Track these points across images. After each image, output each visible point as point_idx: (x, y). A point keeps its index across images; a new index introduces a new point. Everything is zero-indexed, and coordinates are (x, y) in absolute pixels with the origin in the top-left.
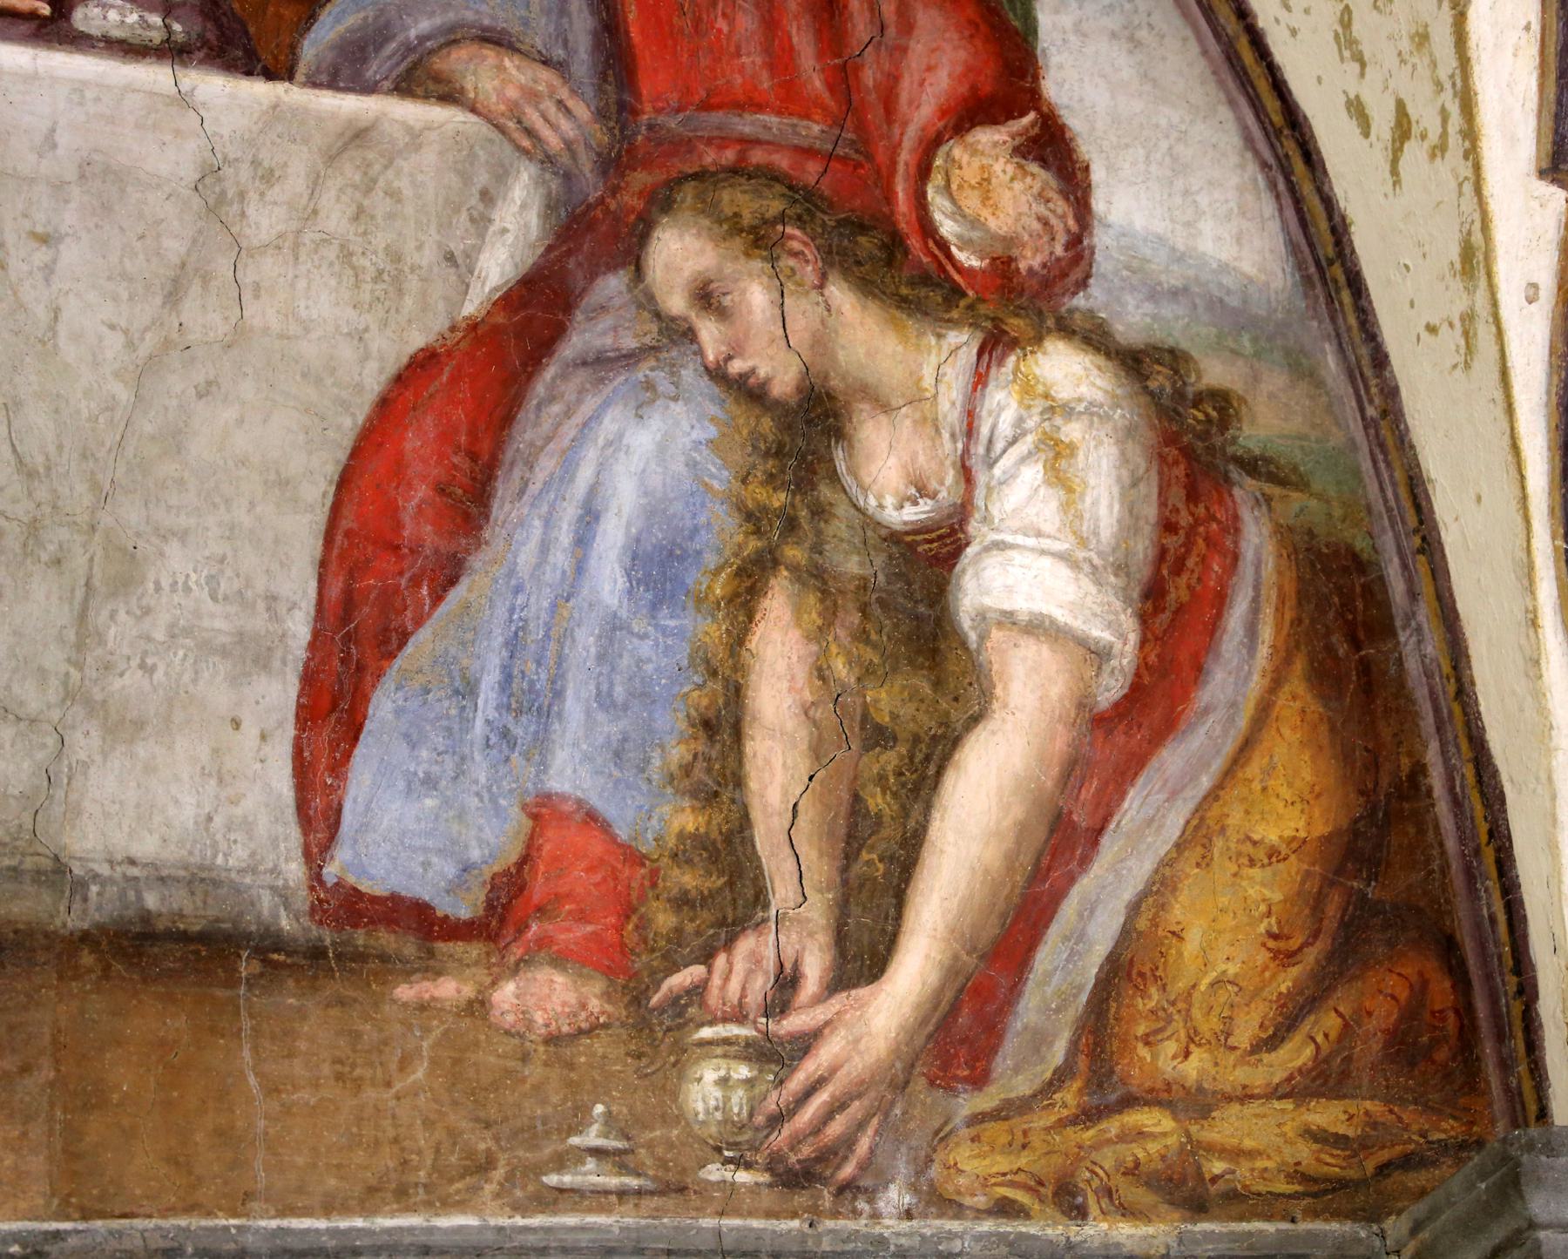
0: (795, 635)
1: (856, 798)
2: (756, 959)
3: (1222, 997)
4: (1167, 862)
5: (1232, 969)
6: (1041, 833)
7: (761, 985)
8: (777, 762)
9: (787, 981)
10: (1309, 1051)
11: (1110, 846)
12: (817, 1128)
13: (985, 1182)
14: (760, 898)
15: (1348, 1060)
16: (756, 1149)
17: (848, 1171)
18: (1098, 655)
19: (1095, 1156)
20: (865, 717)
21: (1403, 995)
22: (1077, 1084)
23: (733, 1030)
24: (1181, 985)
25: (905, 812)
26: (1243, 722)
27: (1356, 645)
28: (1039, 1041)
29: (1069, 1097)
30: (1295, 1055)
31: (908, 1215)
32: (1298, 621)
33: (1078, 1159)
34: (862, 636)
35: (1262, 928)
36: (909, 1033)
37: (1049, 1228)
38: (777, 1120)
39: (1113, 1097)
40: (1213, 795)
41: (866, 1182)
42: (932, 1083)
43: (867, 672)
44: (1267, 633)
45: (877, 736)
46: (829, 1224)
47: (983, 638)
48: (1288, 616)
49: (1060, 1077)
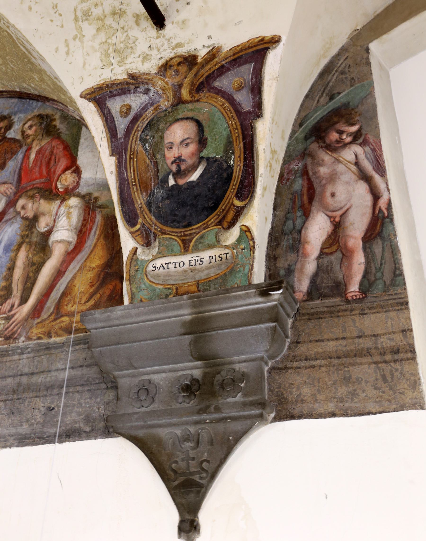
0: (25, 252)
1: (28, 275)
2: (9, 304)
3: (81, 295)
4: (75, 274)
5: (83, 290)
6: (56, 274)
7: (9, 307)
8: (18, 272)
9: (13, 306)
10: (93, 302)
11: (67, 273)
12: (12, 330)
13: (37, 334)
14: (11, 294)
15: (100, 302)
16: (2, 334)
17: (16, 335)
18: (70, 243)
19: (55, 327)
20: (32, 262)
21: (112, 288)
22: (54, 315)
23: (4, 315)
24: (74, 294)
25: (35, 275)
26: (92, 248)
27: (112, 230)
28: (49, 308)
29: (52, 317)
30: (92, 302)
31: (24, 342)
32: (103, 229)
33: (52, 327)
34: (34, 250)
35: (89, 282)
36: (29, 311)
37: (45, 341)
38: (6, 329)
39: (59, 316)
40: (85, 261)
41: (18, 337)
42: (31, 319)
43: (34, 255)
44: (98, 232)
45: (33, 264)
46: (11, 345)
47: (52, 245)
48: (102, 228)
49: (52, 314)
